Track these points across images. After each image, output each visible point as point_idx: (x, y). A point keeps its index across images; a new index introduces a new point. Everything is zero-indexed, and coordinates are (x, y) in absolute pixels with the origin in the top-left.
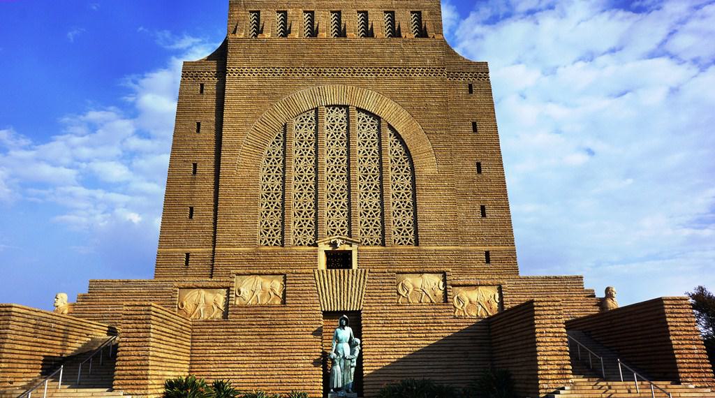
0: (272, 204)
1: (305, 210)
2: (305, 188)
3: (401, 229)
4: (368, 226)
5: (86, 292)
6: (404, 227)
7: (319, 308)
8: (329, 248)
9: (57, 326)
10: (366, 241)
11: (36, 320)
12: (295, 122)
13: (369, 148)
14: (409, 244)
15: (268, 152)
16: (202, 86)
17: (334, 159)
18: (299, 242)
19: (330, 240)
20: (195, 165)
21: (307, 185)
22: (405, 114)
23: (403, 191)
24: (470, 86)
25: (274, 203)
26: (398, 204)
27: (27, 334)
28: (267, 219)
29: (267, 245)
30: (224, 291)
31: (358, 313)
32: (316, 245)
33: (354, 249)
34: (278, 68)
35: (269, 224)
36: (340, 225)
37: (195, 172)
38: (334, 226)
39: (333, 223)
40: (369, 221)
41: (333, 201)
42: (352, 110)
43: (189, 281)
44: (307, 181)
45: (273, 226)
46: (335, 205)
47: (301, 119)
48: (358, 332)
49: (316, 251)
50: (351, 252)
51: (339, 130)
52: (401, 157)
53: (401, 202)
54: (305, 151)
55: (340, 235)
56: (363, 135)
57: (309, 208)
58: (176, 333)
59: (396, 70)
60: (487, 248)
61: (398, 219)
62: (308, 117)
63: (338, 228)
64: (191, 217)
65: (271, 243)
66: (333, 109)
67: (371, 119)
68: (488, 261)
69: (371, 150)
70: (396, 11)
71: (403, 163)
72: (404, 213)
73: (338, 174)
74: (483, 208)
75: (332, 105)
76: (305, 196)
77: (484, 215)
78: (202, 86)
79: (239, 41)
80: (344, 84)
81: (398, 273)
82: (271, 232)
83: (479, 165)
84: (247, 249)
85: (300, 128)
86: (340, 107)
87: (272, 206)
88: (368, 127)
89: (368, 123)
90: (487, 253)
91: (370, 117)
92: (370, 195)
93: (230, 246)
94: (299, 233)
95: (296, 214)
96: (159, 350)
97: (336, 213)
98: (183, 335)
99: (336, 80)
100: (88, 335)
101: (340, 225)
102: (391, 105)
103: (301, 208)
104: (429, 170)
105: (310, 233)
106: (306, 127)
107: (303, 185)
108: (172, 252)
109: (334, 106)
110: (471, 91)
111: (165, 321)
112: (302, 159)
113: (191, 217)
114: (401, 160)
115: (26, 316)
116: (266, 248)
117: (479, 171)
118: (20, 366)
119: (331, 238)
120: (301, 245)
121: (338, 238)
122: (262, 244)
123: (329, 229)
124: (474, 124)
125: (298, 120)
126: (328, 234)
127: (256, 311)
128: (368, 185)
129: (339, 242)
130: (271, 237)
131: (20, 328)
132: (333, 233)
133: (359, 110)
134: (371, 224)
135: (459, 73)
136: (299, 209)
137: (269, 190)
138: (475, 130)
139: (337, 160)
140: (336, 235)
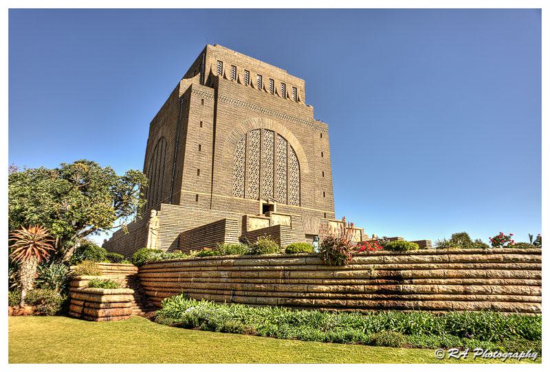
1: (254, 181)
8: (266, 202)
16: (203, 100)
22: (297, 142)
32: (259, 200)
33: (275, 204)
42: (276, 135)
60: (325, 212)
61: (293, 193)
64: (198, 175)
73: (268, 165)
78: (203, 100)
99: (270, 116)
102: (292, 136)
113: (198, 175)
133: (278, 134)
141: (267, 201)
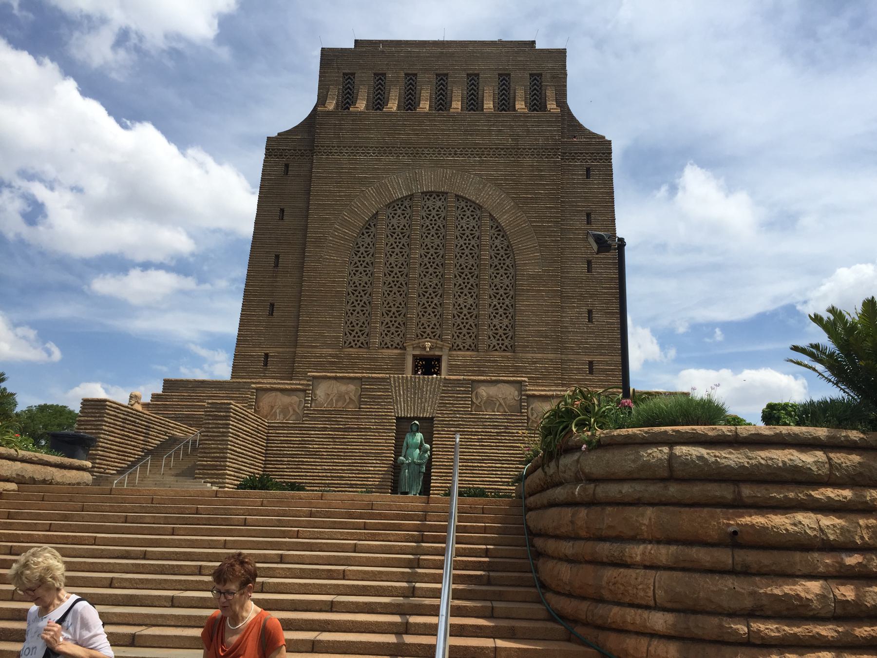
0: (359, 302)
1: (394, 309)
2: (395, 285)
3: (497, 334)
4: (461, 329)
5: (159, 390)
6: (501, 332)
7: (393, 414)
8: (417, 352)
9: (140, 422)
10: (458, 346)
11: (124, 414)
12: (390, 211)
13: (467, 242)
15: (357, 244)
16: (287, 166)
17: (428, 253)
18: (386, 344)
19: (419, 343)
20: (277, 257)
21: (397, 282)
22: (509, 204)
23: (502, 292)
24: (588, 170)
25: (361, 301)
26: (495, 306)
27: (117, 427)
28: (353, 319)
29: (352, 347)
30: (302, 394)
31: (431, 419)
32: (404, 348)
34: (372, 147)
35: (354, 324)
36: (430, 327)
37: (276, 266)
38: (425, 328)
39: (423, 324)
40: (463, 323)
41: (424, 300)
43: (267, 382)
44: (398, 277)
45: (359, 326)
46: (427, 305)
47: (394, 207)
48: (429, 439)
49: (404, 354)
50: (441, 356)
51: (435, 220)
52: (502, 252)
54: (398, 244)
55: (430, 338)
56: (462, 227)
57: (398, 307)
58: (252, 432)
62: (402, 205)
63: (428, 330)
64: (271, 314)
65: (356, 344)
66: (431, 196)
67: (471, 209)
68: (591, 372)
69: (469, 244)
71: (504, 260)
73: (431, 270)
74: (590, 312)
75: (428, 192)
76: (395, 294)
77: (590, 320)
78: (287, 166)
79: (329, 113)
80: (444, 168)
81: (473, 381)
82: (357, 333)
85: (393, 217)
86: (439, 194)
87: (359, 304)
88: (468, 217)
89: (468, 213)
90: (591, 363)
91: (470, 206)
92: (466, 295)
94: (386, 335)
95: (385, 314)
96: (236, 445)
97: (427, 314)
98: (259, 435)
100: (166, 432)
101: (430, 327)
103: (390, 307)
105: (399, 335)
106: (399, 216)
107: (393, 282)
109: (430, 193)
111: (243, 419)
112: (393, 252)
113: (271, 314)
114: (502, 256)
115: (117, 411)
116: (351, 350)
118: (111, 455)
119: (420, 340)
120: (388, 348)
122: (346, 345)
123: (419, 331)
124: (588, 215)
125: (391, 208)
126: (417, 336)
127: (328, 415)
128: (464, 283)
129: (428, 345)
130: (356, 339)
131: (112, 421)
132: (422, 336)
133: (458, 197)
134: (465, 327)
135: (576, 153)
136: (387, 309)
137: (356, 286)
139: (432, 255)
140: (426, 338)
141: (425, 348)
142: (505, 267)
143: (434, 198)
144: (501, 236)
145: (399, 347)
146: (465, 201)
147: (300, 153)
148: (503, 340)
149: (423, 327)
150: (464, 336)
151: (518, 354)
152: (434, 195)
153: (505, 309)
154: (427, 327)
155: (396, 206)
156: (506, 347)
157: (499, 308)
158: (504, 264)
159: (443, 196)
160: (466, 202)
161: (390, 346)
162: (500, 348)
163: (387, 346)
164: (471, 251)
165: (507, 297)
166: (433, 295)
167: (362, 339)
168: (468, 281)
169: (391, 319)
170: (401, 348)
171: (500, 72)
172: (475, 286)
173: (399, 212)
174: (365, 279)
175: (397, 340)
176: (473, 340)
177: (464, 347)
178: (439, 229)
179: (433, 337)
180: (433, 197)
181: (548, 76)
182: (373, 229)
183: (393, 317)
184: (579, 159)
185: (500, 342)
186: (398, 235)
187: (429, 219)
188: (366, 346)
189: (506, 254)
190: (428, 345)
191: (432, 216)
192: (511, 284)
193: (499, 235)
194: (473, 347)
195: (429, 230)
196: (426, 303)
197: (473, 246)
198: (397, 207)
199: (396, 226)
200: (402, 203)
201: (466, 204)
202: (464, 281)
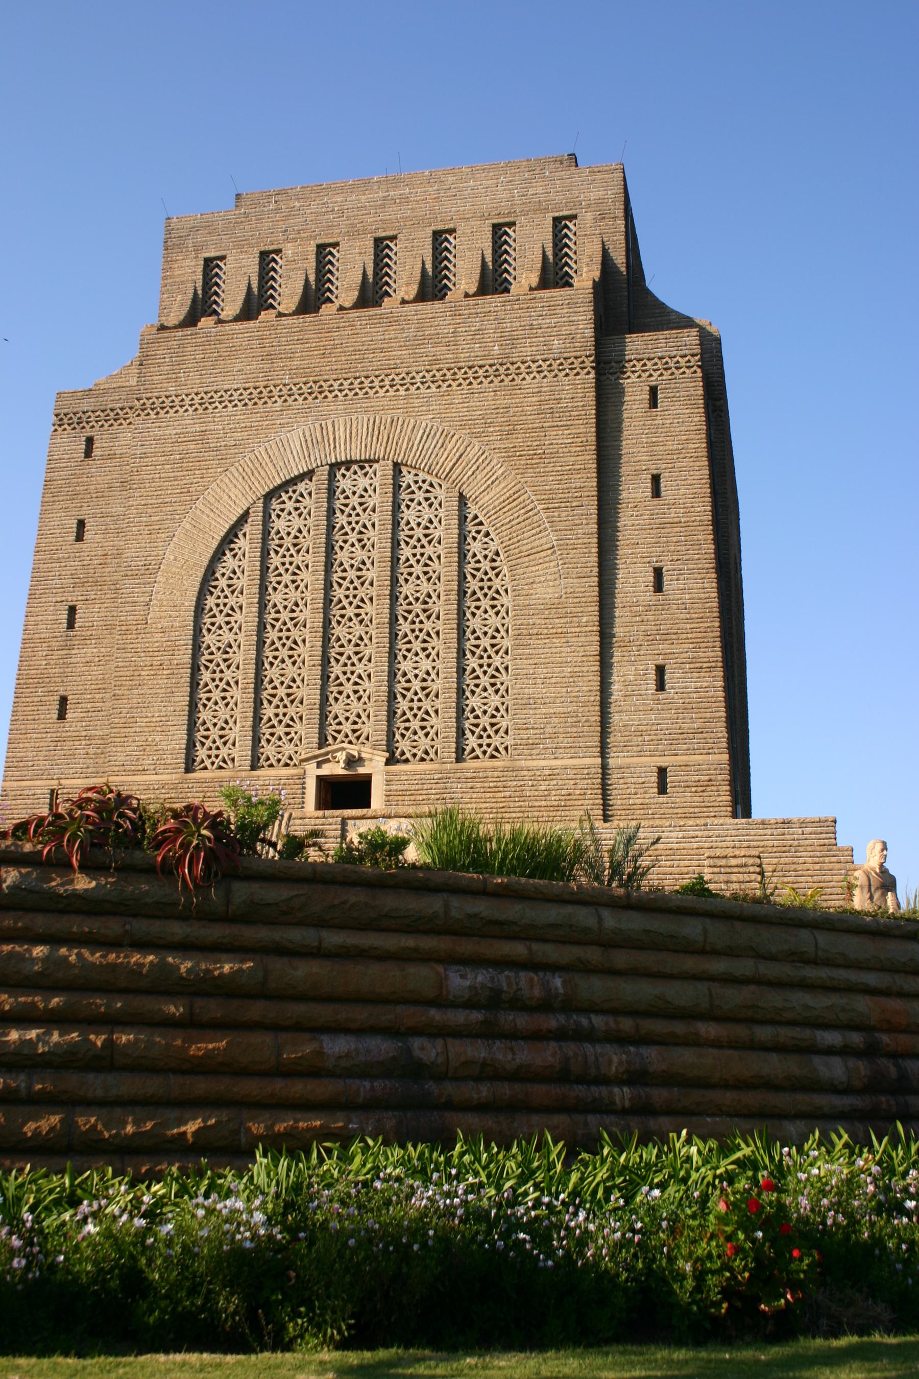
6: (485, 721)
8: (326, 770)
14: (493, 757)
16: (90, 441)
20: (72, 610)
24: (653, 391)
37: (71, 625)
52: (485, 565)
53: (481, 666)
55: (350, 742)
59: (481, 372)
60: (663, 762)
62: (294, 492)
64: (62, 716)
66: (348, 469)
67: (425, 486)
68: (662, 789)
70: (522, 220)
72: (485, 690)
73: (350, 611)
74: (660, 670)
77: (661, 686)
78: (90, 441)
83: (658, 573)
84: (168, 777)
86: (362, 464)
87: (217, 686)
91: (424, 482)
93: (135, 773)
104: (545, 592)
105: (291, 740)
108: (29, 788)
109: (348, 464)
110: (653, 403)
113: (62, 716)
117: (658, 586)
120: (271, 766)
121: (343, 749)
124: (656, 479)
128: (413, 631)
132: (335, 738)
138: (656, 493)
142: (491, 593)
143: (355, 473)
144: (482, 533)
145: (292, 763)
146: (413, 472)
147: (112, 414)
148: (489, 737)
149: (336, 721)
150: (415, 733)
151: (518, 763)
152: (355, 467)
153: (493, 677)
154: (343, 721)
155: (283, 494)
156: (497, 749)
157: (481, 675)
158: (490, 588)
159: (371, 467)
160: (416, 475)
161: (275, 763)
162: (485, 752)
163: (268, 763)
164: (425, 569)
165: (497, 652)
166: (355, 659)
167: (224, 752)
168: (421, 626)
169: (277, 711)
170: (295, 765)
171: (495, 221)
172: (434, 636)
173: (290, 505)
174: (228, 637)
175: (289, 749)
176: (433, 740)
177: (415, 755)
178: (363, 530)
179: (354, 741)
180: (352, 470)
181: (589, 216)
182: (242, 543)
183: (281, 706)
184: (633, 372)
185: (485, 741)
186: (288, 550)
187: (346, 513)
188: (231, 765)
189: (493, 569)
190: (342, 756)
191: (350, 506)
192: (503, 625)
193: (478, 532)
194: (432, 755)
195: (346, 534)
196: (341, 675)
197: (430, 558)
198: (285, 497)
199: (283, 534)
200: (295, 488)
201: (416, 478)
202: (413, 626)
